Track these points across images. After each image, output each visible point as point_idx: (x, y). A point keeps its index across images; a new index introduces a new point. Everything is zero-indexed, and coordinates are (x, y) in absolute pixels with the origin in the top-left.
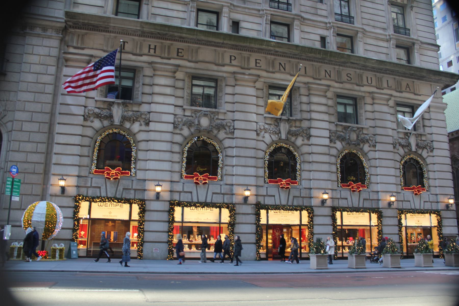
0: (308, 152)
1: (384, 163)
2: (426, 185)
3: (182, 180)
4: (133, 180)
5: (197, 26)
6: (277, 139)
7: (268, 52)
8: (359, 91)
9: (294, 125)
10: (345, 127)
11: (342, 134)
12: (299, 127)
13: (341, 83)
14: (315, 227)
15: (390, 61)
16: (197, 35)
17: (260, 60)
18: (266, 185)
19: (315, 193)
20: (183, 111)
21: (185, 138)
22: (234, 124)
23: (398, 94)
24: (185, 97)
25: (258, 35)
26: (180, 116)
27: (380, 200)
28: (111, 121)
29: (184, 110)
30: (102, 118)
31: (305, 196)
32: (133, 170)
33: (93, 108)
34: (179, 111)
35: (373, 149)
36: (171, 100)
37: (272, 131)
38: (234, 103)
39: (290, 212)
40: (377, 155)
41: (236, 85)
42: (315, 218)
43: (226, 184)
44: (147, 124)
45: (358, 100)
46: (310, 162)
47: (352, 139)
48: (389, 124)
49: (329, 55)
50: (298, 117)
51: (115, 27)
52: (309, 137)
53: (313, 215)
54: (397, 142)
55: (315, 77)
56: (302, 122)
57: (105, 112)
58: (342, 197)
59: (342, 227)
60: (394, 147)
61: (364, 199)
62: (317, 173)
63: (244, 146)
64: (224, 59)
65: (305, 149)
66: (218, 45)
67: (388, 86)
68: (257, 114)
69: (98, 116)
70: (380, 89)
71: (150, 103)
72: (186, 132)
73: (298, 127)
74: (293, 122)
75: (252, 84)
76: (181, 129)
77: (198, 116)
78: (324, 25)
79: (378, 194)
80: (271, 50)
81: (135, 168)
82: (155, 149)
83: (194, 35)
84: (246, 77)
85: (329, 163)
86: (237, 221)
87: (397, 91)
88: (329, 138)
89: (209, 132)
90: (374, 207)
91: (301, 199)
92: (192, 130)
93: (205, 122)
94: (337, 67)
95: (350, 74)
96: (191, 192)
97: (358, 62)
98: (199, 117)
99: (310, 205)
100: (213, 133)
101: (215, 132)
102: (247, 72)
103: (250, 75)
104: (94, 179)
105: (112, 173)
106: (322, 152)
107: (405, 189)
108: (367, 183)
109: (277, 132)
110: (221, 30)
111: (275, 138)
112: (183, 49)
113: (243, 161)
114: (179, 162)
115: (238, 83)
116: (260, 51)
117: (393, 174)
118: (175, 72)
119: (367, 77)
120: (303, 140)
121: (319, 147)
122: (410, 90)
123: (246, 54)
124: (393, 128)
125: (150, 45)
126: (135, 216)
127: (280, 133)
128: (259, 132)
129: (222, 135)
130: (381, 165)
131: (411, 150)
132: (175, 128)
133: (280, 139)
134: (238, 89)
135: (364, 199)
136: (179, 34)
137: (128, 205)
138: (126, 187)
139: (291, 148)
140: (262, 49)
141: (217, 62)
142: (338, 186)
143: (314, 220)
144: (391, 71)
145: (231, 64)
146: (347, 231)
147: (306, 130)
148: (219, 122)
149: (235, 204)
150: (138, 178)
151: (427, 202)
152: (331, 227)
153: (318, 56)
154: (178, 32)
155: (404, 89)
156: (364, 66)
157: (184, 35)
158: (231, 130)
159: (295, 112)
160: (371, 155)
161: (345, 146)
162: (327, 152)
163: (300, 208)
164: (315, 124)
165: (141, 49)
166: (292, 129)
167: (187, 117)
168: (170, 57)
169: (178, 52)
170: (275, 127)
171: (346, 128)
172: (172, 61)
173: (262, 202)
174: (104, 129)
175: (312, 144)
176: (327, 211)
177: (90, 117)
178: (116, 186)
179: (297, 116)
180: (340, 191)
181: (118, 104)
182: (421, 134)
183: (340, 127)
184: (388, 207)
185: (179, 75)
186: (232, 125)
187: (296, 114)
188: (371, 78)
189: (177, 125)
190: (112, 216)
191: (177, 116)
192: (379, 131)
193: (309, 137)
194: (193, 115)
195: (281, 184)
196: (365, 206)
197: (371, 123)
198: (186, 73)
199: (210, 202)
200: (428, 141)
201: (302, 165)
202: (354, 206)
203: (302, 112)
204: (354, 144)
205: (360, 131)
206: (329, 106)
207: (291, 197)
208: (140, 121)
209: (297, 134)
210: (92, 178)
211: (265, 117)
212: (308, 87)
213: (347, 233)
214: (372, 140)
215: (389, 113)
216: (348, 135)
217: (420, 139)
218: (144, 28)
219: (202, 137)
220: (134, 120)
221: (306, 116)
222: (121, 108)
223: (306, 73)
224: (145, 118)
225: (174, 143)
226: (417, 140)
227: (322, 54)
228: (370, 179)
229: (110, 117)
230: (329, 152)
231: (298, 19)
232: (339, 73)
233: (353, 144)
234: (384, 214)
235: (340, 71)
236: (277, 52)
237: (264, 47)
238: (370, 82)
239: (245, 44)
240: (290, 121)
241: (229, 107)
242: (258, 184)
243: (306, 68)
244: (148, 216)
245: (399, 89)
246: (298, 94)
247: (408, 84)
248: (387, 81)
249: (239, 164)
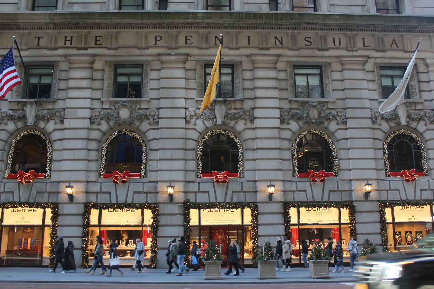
0: (251, 138)
1: (357, 144)
2: (426, 168)
3: (100, 180)
4: (47, 183)
5: (207, 9)
6: (212, 125)
7: (199, 26)
8: (323, 57)
9: (233, 107)
10: (302, 103)
11: (298, 111)
12: (241, 108)
13: (298, 50)
14: (260, 227)
15: (368, 14)
16: (111, 18)
17: (191, 36)
18: (198, 180)
19: (260, 186)
20: (101, 104)
21: (104, 134)
22: (159, 112)
23: (379, 54)
24: (105, 88)
25: (189, 8)
26: (97, 110)
27: (353, 191)
28: (25, 122)
29: (102, 102)
30: (16, 120)
31: (248, 190)
32: (48, 172)
33: (6, 110)
34: (97, 105)
35: (342, 126)
36: (88, 93)
37: (205, 117)
38: (159, 89)
39: (229, 211)
40: (349, 133)
41: (162, 68)
42: (260, 217)
43: (150, 182)
44: (62, 122)
45: (323, 68)
46: (255, 150)
47: (311, 116)
48: (365, 94)
49: (274, 18)
50: (239, 96)
51: (23, 22)
52: (253, 119)
53: (258, 214)
54: (377, 115)
55: (261, 46)
56: (245, 102)
57: (19, 113)
58: (298, 190)
59: (299, 227)
61: (330, 191)
62: (263, 161)
63: (171, 137)
64: (147, 42)
65: (248, 134)
66: (139, 26)
67: (364, 46)
68: (186, 99)
69: (11, 118)
70: (352, 50)
71: (64, 99)
72: (104, 126)
73: (239, 109)
74: (233, 104)
75: (181, 65)
76: (99, 124)
77: (117, 108)
79: (351, 183)
80: (201, 23)
81: (50, 170)
82: (70, 148)
83: (108, 19)
84: (173, 57)
85: (280, 149)
86: (161, 223)
87: (377, 51)
88: (279, 118)
89: (130, 124)
90: (344, 199)
91: (242, 194)
92: (111, 123)
93: (124, 114)
94: (290, 31)
95: (310, 38)
96: (110, 193)
97: (315, 21)
98: (119, 108)
99: (255, 201)
100: (135, 125)
101: (137, 123)
102: (173, 52)
103: (176, 54)
104: (7, 184)
105: (25, 177)
106: (269, 136)
107: (392, 175)
108: (336, 171)
109: (211, 117)
110: (234, 9)
111: (209, 124)
112: (102, 37)
113: (168, 154)
114: (97, 160)
115: (164, 66)
116: (188, 25)
117: (371, 157)
118: (92, 63)
119: (334, 38)
122: (398, 47)
123: (173, 31)
124: (372, 98)
125: (66, 37)
126: (48, 222)
127: (215, 117)
128: (188, 119)
129: (145, 126)
130: (353, 147)
131: (399, 124)
132: (92, 123)
133: (215, 125)
134: (164, 73)
135: (330, 191)
136: (92, 21)
137: (42, 210)
138: (40, 191)
139: (231, 135)
140: (190, 24)
141: (140, 45)
142: (294, 177)
143: (259, 219)
144: (366, 26)
145: (156, 45)
146: (315, 231)
147: (249, 111)
148: (142, 111)
149: (158, 203)
150: (52, 179)
151: (426, 190)
152: (282, 228)
153: (259, 21)
154: (91, 19)
155: (388, 47)
156: (325, 25)
157: (97, 21)
158: (156, 119)
159: (237, 92)
160: (340, 134)
161: (303, 126)
162: (277, 135)
163: (242, 206)
165: (56, 42)
166: (230, 112)
167: (105, 111)
168: (87, 46)
169: (96, 40)
170: (210, 111)
171: (303, 104)
172: (90, 51)
173: (191, 201)
174: (18, 130)
175: (256, 128)
176: (278, 208)
177: (4, 120)
178: (30, 190)
179: (239, 96)
180: (296, 182)
181: (31, 103)
182: (414, 102)
183: (296, 103)
184: (364, 199)
185: (98, 65)
186: (157, 113)
187: (238, 94)
188: (340, 39)
189: (94, 120)
190: (24, 222)
191: (95, 110)
192: (350, 103)
194: (112, 107)
195: (217, 177)
196: (331, 199)
197: (339, 95)
198: (106, 62)
199: (131, 202)
200: (426, 110)
201: (245, 154)
202: (316, 199)
203: (245, 91)
204: (315, 123)
205: (323, 106)
206: (280, 80)
207: (230, 193)
208: (54, 119)
209: (237, 118)
210: (5, 183)
211: (197, 101)
212: (252, 60)
213: (315, 233)
214: (341, 116)
215: (366, 80)
216: (305, 112)
217: (414, 108)
218: (53, 19)
219: (123, 131)
220: (48, 119)
221: (249, 94)
222: (34, 107)
223: (249, 44)
224: (60, 116)
225: (90, 140)
226: (407, 110)
227: (264, 18)
228: (339, 164)
229: (24, 118)
230: (280, 135)
232: (294, 38)
233: (313, 123)
234: (358, 208)
235: (295, 36)
236: (208, 23)
237: (190, 21)
238: (337, 43)
239: (167, 21)
240: (227, 102)
241: (153, 94)
242: (188, 179)
243: (250, 38)
244: (61, 220)
245: (381, 47)
246: (240, 70)
247: (394, 40)
248: (363, 39)
249: (164, 158)
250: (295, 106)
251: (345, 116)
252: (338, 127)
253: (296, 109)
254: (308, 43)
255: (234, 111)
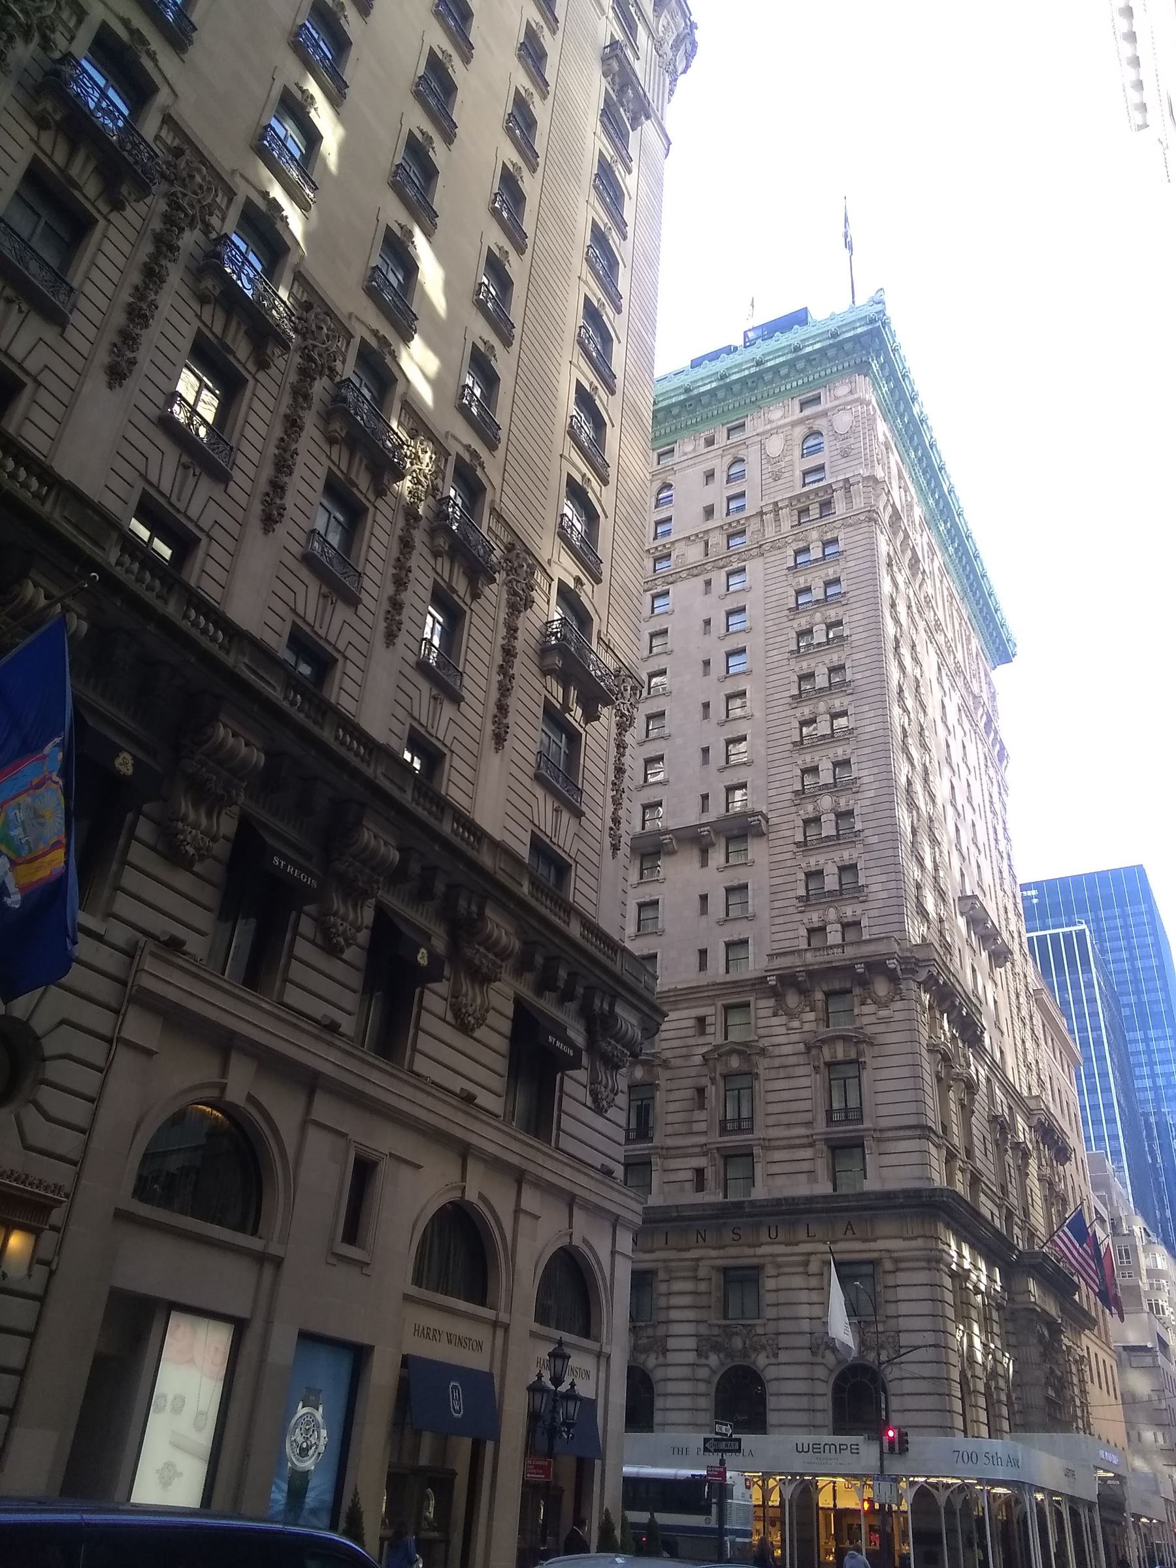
8: (755, 1256)
11: (720, 1339)
35: (773, 1361)
48: (804, 1311)
52: (665, 1351)
60: (814, 1354)
78: (697, 1150)
120: (657, 1359)
121: (679, 1368)
164: (676, 1329)
166: (639, 1342)
192: (784, 1326)
193: (665, 1351)
206: (699, 1294)
231: (657, 1153)
238: (773, 1235)
250: (716, 1331)
251: (777, 1345)
252: (767, 1361)
253: (719, 1335)
254: (736, 1237)
255: (644, 1341)
